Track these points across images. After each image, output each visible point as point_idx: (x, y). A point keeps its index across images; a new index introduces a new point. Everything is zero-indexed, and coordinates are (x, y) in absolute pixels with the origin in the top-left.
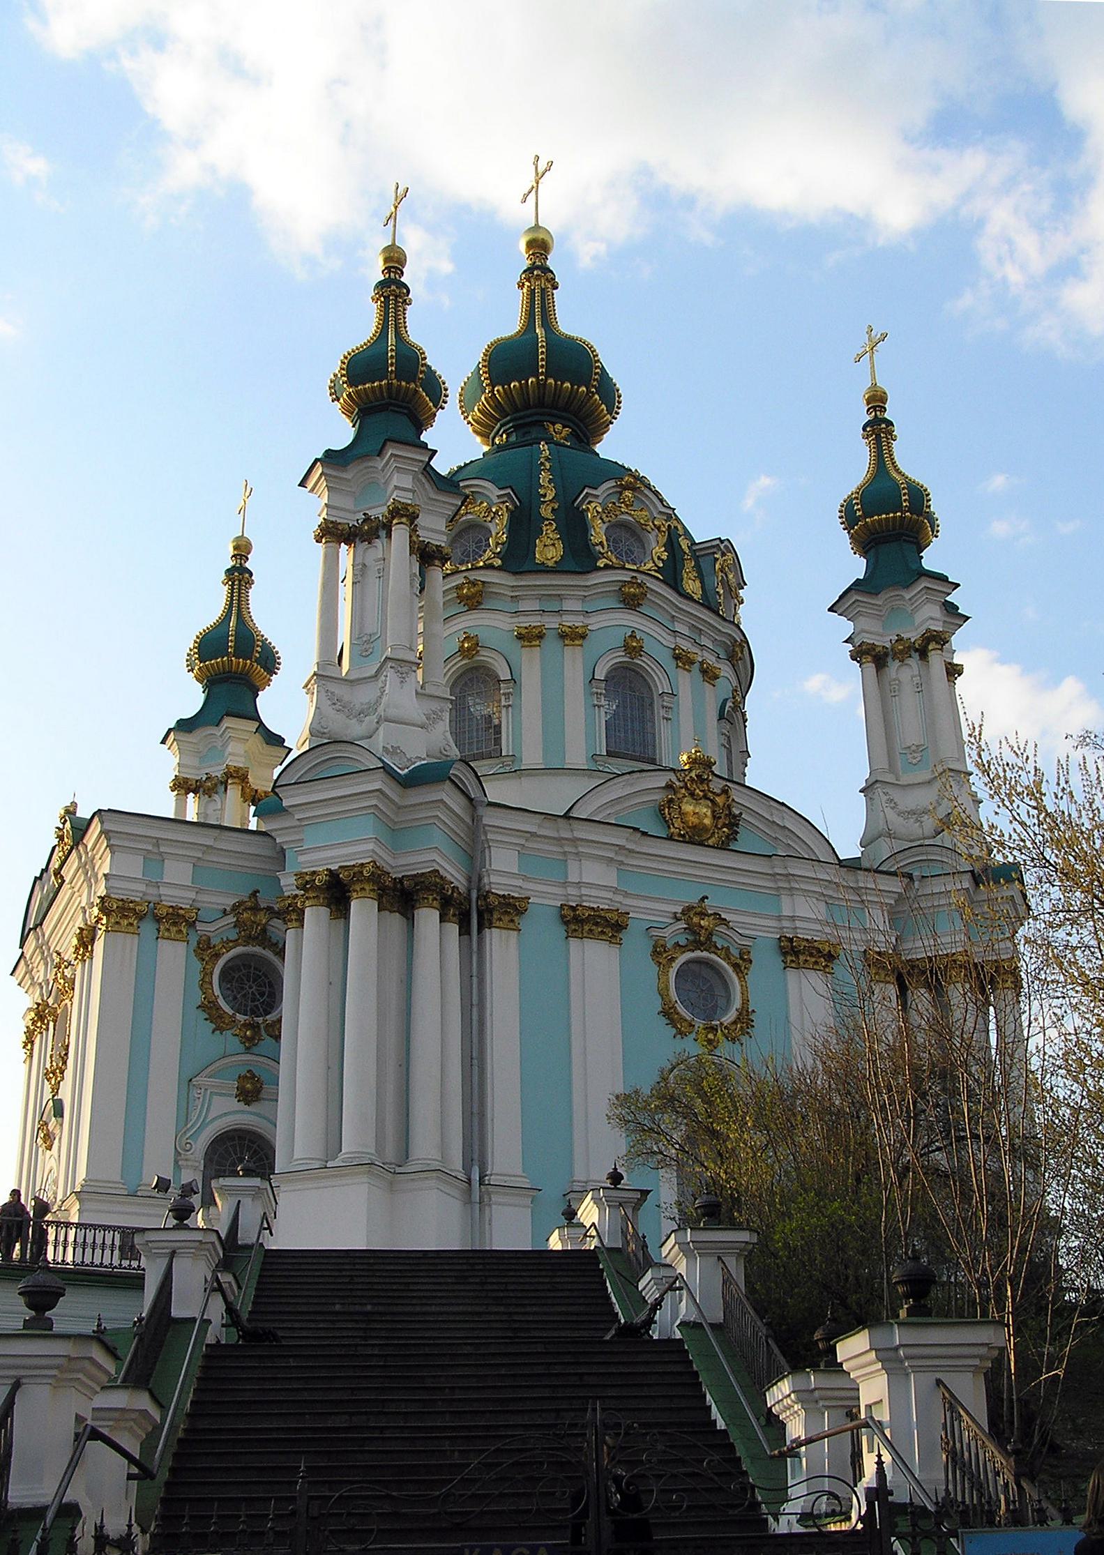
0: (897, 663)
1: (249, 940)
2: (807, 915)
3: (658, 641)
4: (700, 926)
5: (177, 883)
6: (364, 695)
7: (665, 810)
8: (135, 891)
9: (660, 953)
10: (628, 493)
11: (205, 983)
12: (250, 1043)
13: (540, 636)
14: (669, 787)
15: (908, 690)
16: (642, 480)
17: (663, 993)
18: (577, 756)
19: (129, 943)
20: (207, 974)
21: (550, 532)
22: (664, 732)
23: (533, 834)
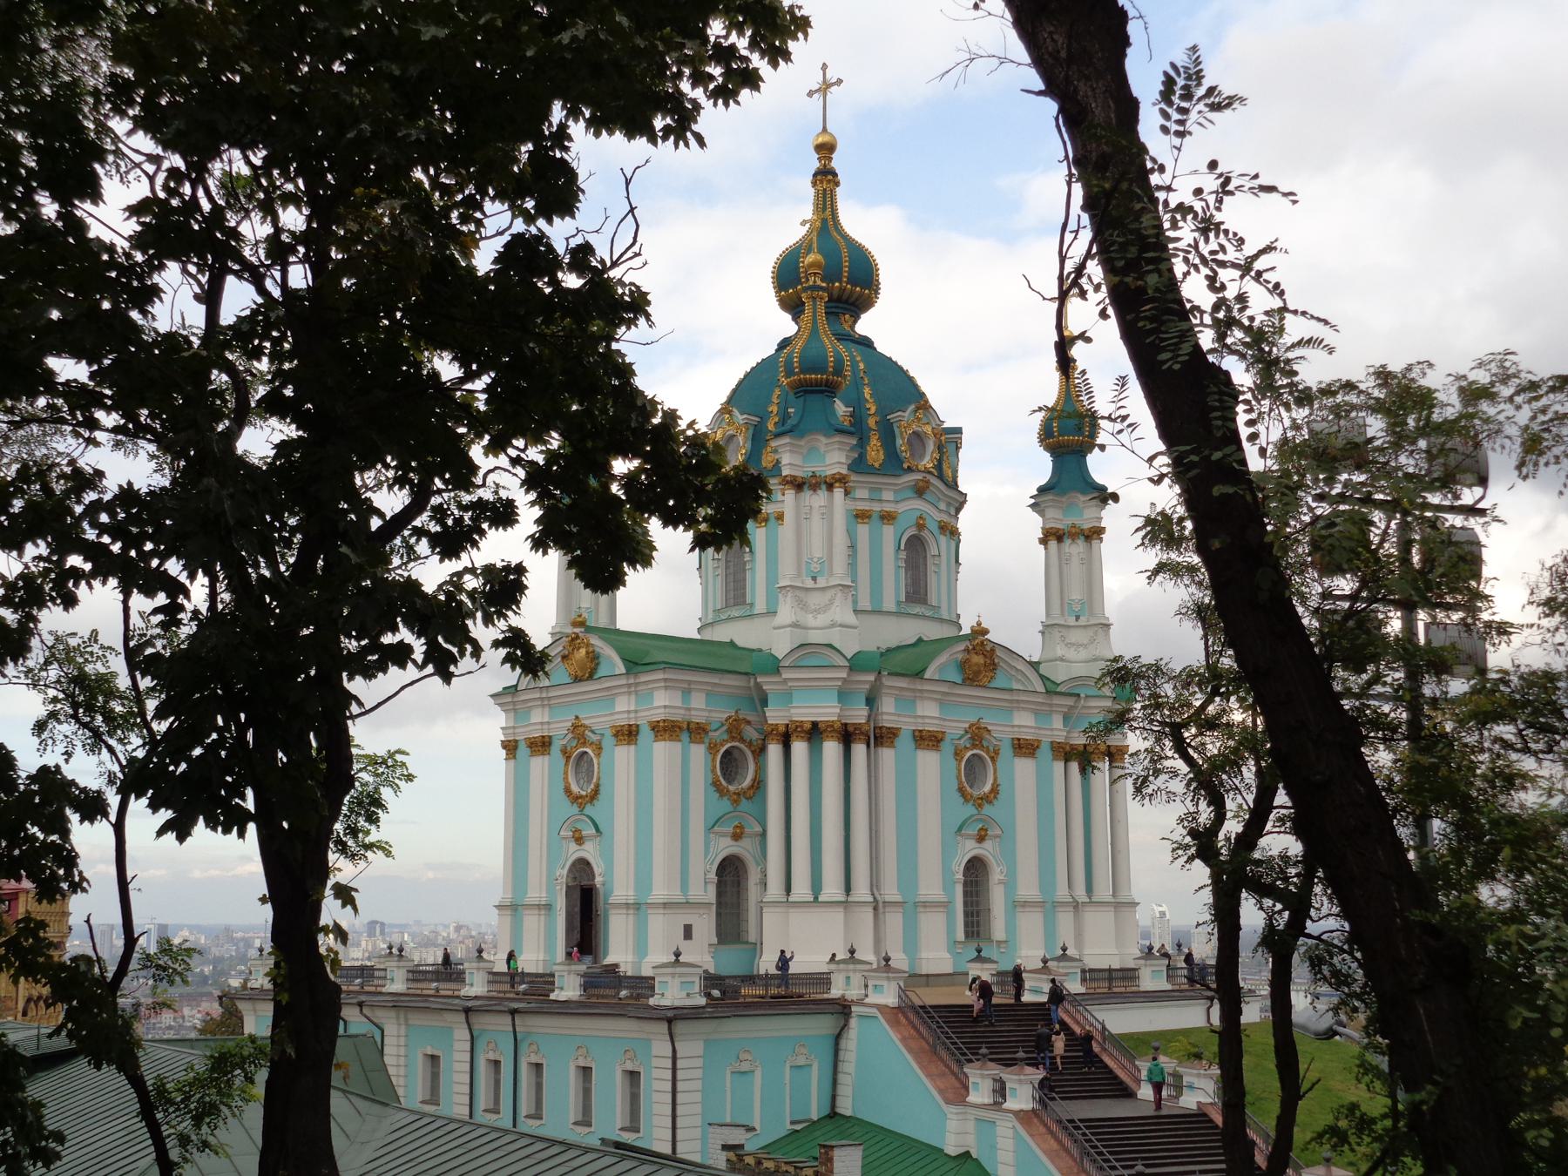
0: (1068, 542)
1: (733, 739)
2: (1024, 723)
3: (934, 516)
4: (977, 734)
5: (700, 707)
6: (815, 600)
7: (963, 665)
8: (678, 715)
9: (958, 754)
10: (920, 414)
11: (713, 771)
12: (736, 802)
13: (869, 517)
14: (967, 650)
15: (1075, 561)
16: (911, 380)
17: (959, 777)
18: (889, 604)
19: (679, 745)
20: (714, 760)
21: (874, 441)
22: (932, 581)
23: (902, 689)
